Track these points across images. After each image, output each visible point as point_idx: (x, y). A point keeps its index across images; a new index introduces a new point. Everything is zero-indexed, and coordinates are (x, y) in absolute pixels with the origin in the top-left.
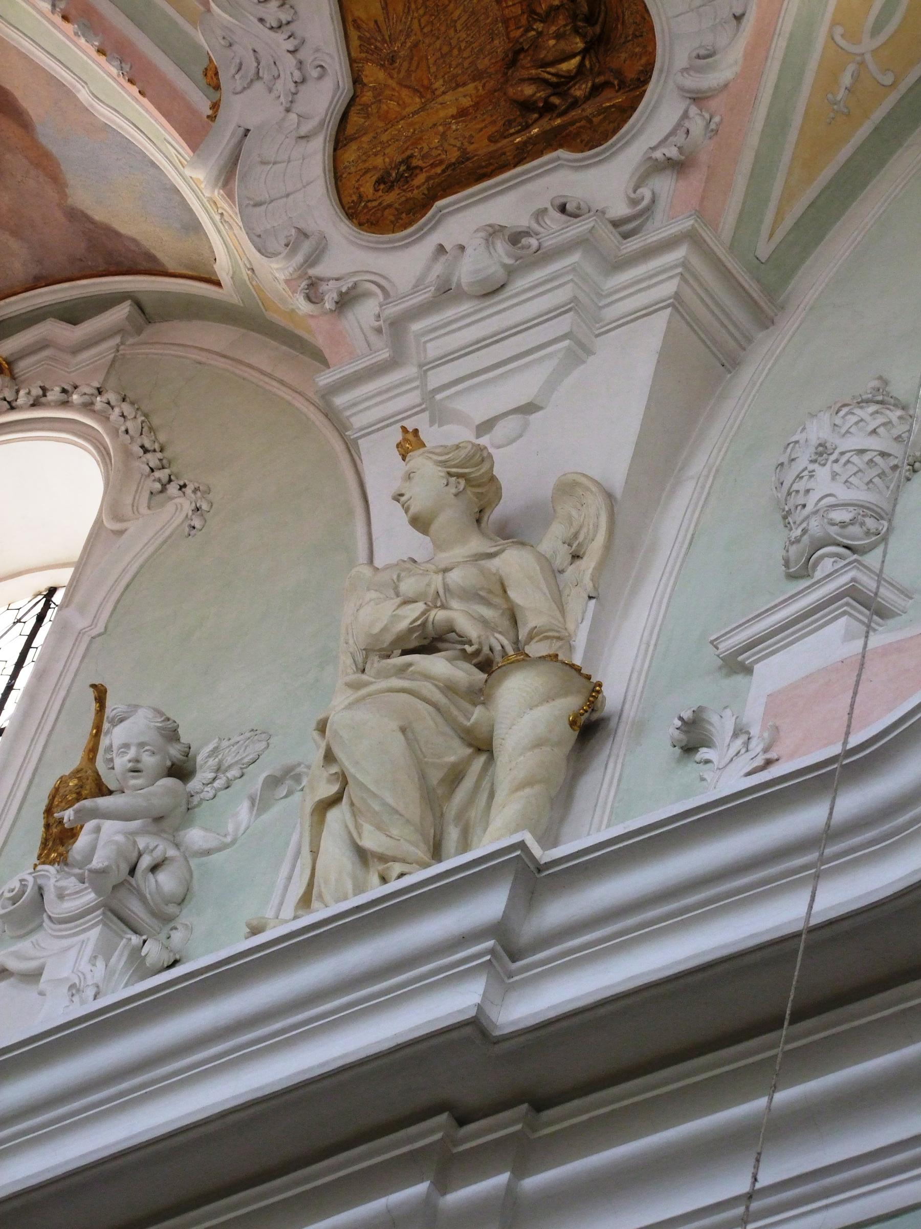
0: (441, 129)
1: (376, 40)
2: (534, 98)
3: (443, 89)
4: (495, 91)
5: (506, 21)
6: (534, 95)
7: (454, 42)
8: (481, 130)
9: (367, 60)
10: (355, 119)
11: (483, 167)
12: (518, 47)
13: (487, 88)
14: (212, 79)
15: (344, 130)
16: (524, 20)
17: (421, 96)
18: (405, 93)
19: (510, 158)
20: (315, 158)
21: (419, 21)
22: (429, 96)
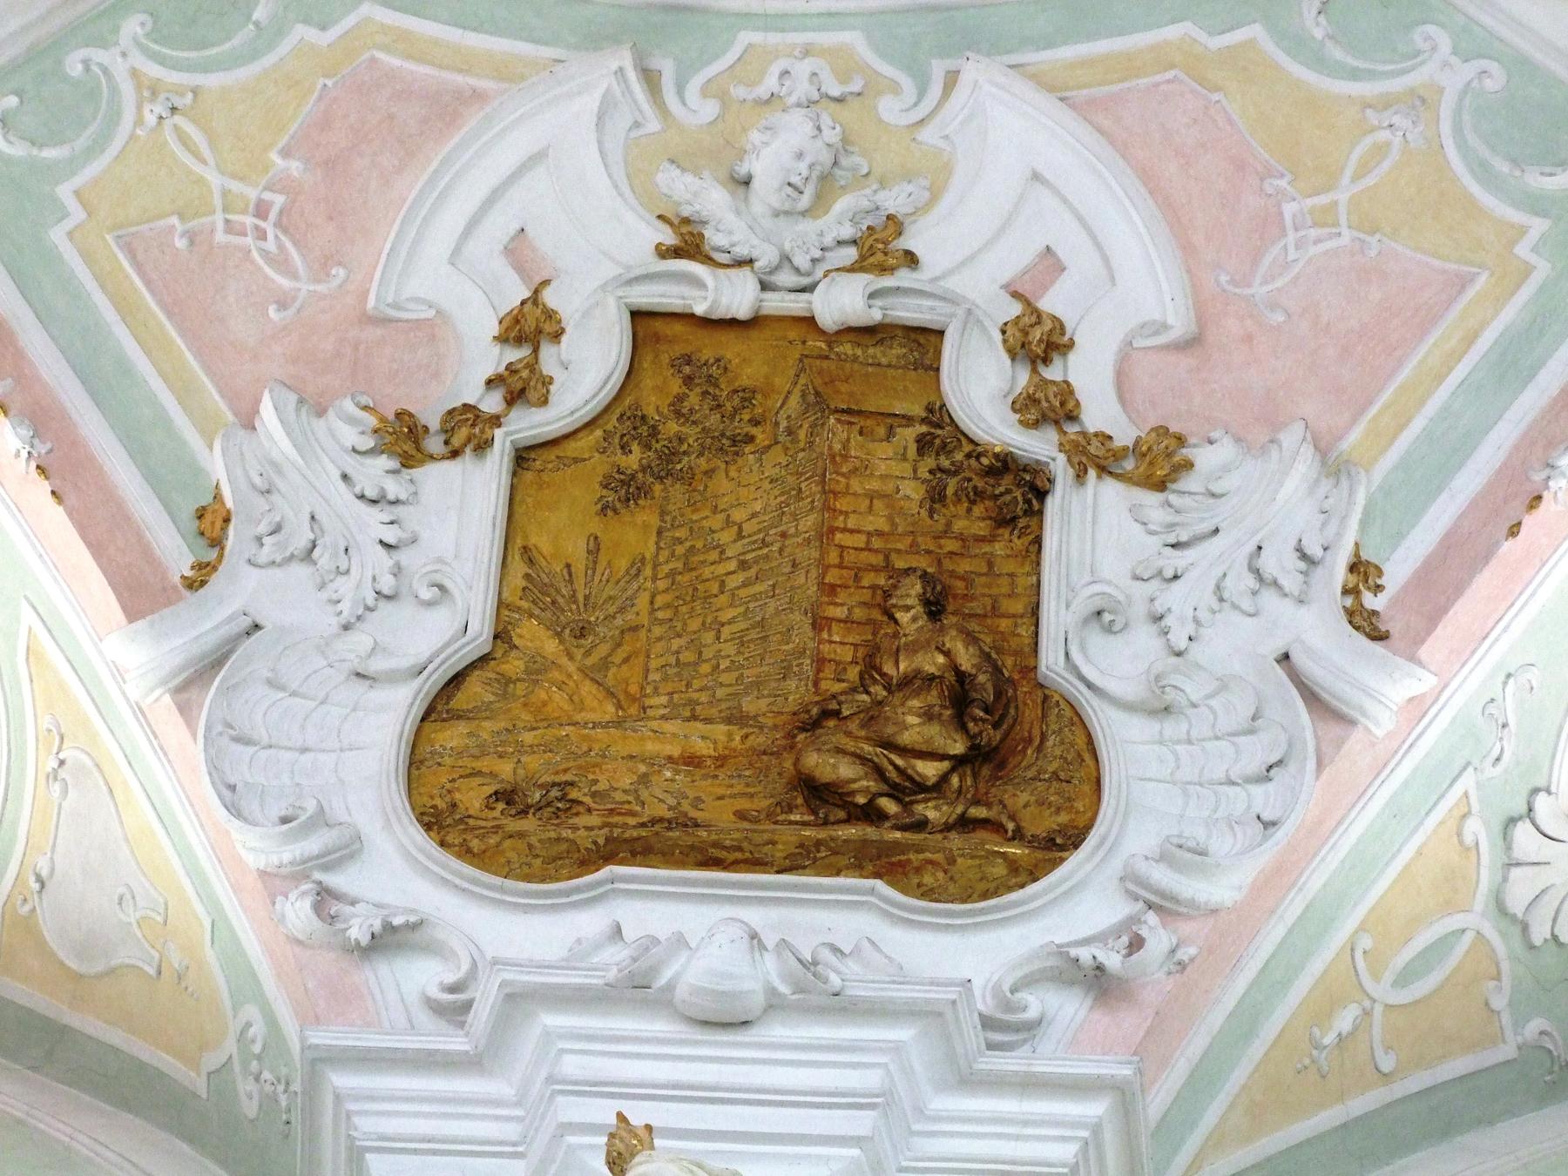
0: (643, 768)
1: (558, 591)
2: (855, 786)
3: (662, 711)
4: (765, 753)
5: (820, 662)
6: (855, 781)
7: (708, 653)
8: (721, 798)
9: (531, 615)
10: (475, 691)
11: (724, 848)
12: (833, 706)
13: (749, 742)
14: (211, 525)
15: (449, 699)
16: (853, 673)
17: (619, 706)
18: (588, 688)
19: (778, 855)
20: (390, 715)
21: (653, 597)
22: (633, 710)
